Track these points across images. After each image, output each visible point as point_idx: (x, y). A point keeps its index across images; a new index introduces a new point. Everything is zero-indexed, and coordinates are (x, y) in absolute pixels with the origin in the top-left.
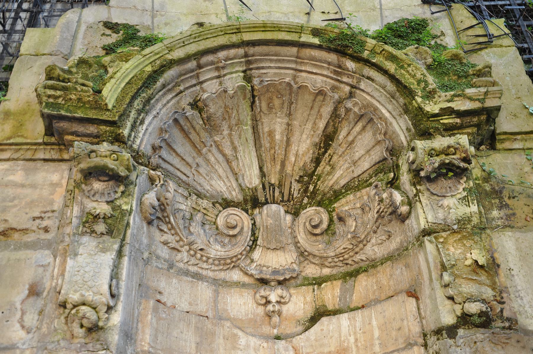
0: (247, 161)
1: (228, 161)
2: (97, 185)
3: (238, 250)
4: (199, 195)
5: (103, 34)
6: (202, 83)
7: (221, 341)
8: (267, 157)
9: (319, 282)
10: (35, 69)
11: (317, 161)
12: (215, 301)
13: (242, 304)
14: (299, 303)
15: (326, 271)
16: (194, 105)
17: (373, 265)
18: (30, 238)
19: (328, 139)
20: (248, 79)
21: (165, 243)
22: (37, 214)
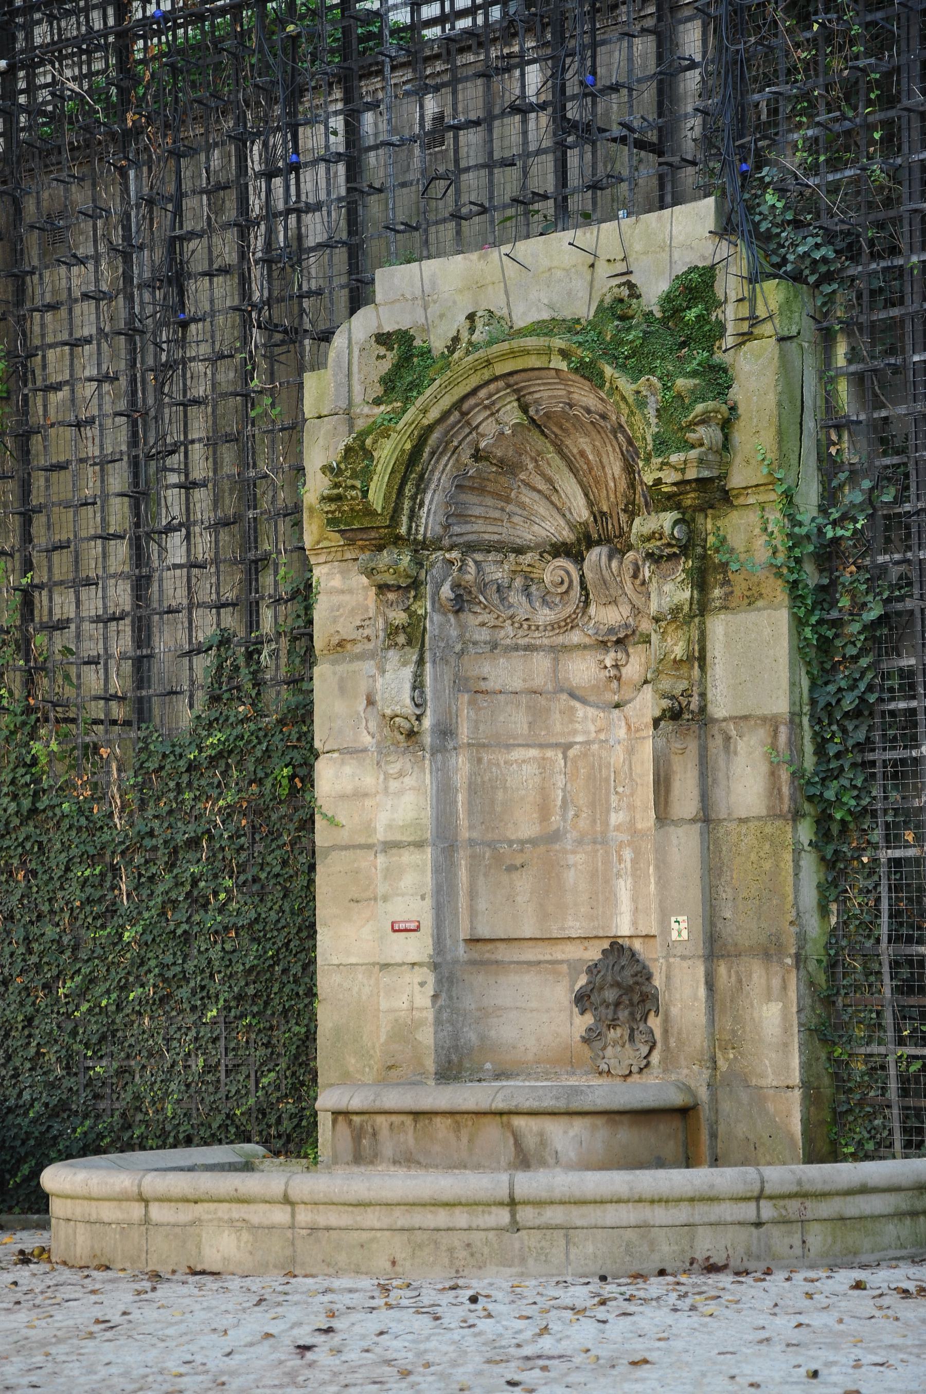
0: (569, 491)
1: (548, 498)
3: (570, 609)
4: (520, 551)
5: (379, 357)
6: (477, 427)
7: (558, 716)
10: (321, 442)
12: (555, 671)
13: (583, 670)
18: (358, 649)
20: (524, 409)
21: (483, 624)
22: (359, 623)
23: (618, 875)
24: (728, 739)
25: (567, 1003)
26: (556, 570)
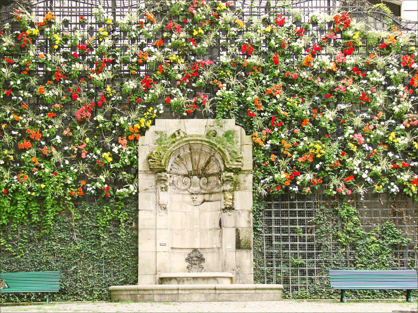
2: (162, 181)
4: (179, 175)
8: (194, 164)
9: (204, 194)
11: (206, 166)
13: (188, 198)
14: (200, 198)
15: (206, 192)
16: (179, 157)
17: (215, 193)
19: (208, 162)
20: (190, 150)
23: (196, 237)
24: (239, 213)
26: (187, 179)
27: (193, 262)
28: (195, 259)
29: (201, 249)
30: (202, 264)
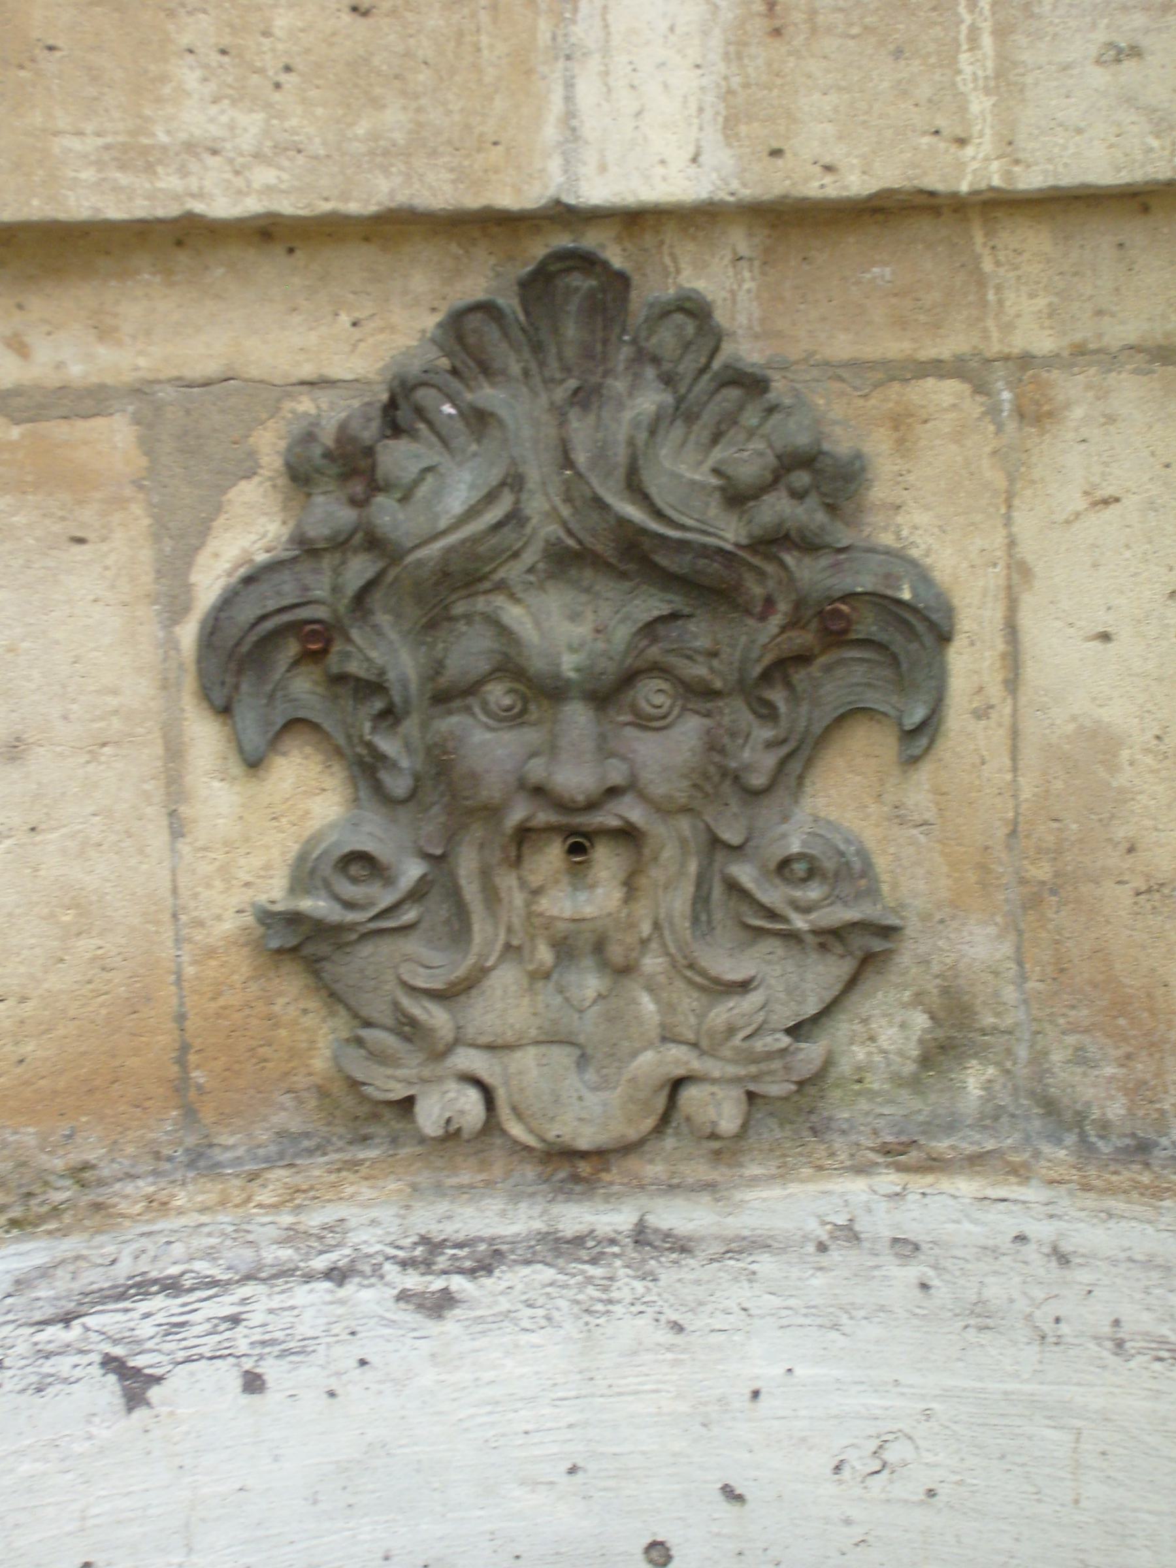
25: (139, 691)
27: (492, 748)
28: (562, 627)
29: (789, 223)
30: (848, 798)
